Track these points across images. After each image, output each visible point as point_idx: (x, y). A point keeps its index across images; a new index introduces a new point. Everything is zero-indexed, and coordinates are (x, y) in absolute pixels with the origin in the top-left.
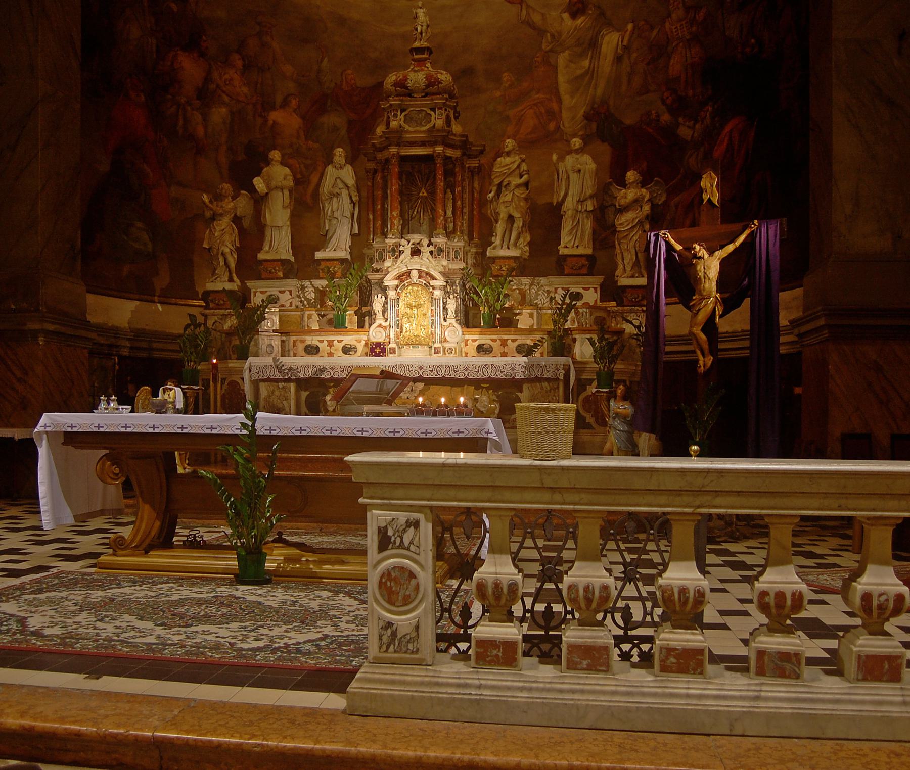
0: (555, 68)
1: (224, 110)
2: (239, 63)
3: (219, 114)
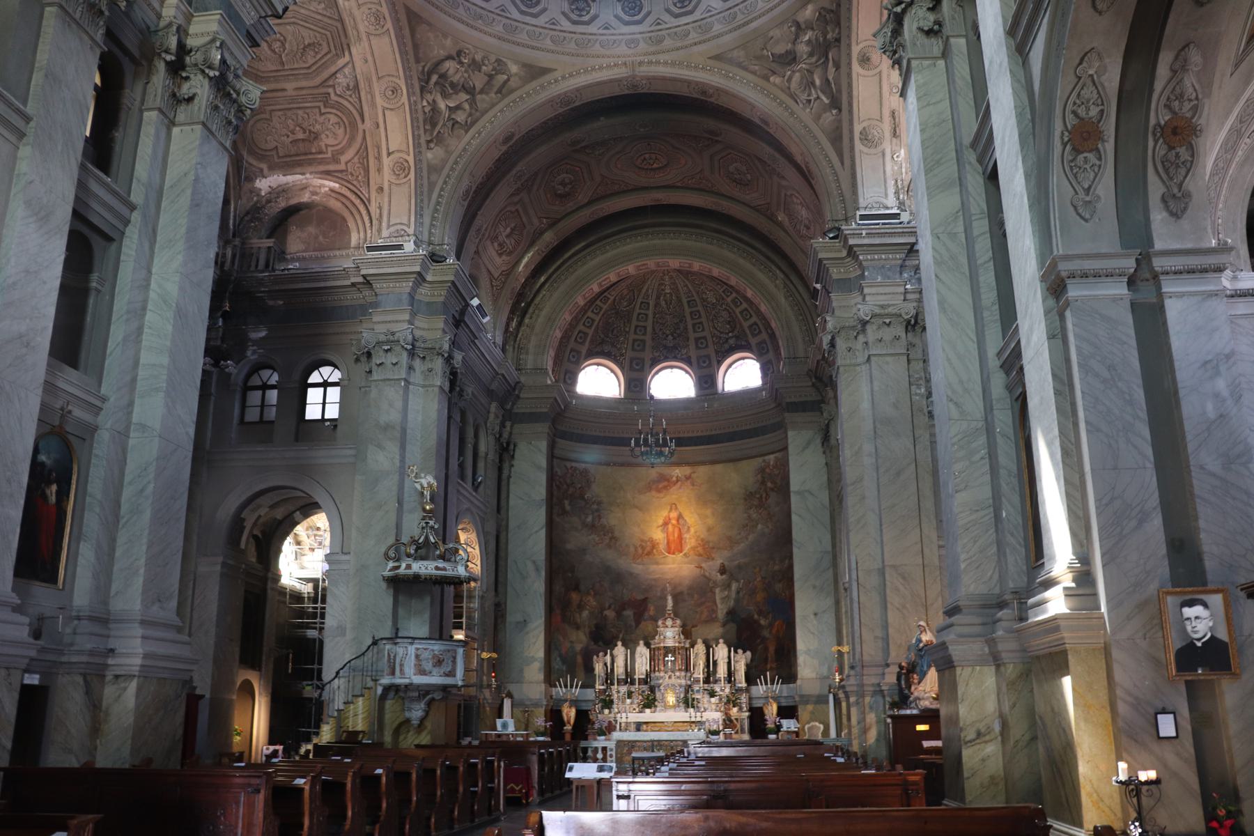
0: (714, 593)
1: (587, 612)
2: (592, 593)
3: (585, 614)
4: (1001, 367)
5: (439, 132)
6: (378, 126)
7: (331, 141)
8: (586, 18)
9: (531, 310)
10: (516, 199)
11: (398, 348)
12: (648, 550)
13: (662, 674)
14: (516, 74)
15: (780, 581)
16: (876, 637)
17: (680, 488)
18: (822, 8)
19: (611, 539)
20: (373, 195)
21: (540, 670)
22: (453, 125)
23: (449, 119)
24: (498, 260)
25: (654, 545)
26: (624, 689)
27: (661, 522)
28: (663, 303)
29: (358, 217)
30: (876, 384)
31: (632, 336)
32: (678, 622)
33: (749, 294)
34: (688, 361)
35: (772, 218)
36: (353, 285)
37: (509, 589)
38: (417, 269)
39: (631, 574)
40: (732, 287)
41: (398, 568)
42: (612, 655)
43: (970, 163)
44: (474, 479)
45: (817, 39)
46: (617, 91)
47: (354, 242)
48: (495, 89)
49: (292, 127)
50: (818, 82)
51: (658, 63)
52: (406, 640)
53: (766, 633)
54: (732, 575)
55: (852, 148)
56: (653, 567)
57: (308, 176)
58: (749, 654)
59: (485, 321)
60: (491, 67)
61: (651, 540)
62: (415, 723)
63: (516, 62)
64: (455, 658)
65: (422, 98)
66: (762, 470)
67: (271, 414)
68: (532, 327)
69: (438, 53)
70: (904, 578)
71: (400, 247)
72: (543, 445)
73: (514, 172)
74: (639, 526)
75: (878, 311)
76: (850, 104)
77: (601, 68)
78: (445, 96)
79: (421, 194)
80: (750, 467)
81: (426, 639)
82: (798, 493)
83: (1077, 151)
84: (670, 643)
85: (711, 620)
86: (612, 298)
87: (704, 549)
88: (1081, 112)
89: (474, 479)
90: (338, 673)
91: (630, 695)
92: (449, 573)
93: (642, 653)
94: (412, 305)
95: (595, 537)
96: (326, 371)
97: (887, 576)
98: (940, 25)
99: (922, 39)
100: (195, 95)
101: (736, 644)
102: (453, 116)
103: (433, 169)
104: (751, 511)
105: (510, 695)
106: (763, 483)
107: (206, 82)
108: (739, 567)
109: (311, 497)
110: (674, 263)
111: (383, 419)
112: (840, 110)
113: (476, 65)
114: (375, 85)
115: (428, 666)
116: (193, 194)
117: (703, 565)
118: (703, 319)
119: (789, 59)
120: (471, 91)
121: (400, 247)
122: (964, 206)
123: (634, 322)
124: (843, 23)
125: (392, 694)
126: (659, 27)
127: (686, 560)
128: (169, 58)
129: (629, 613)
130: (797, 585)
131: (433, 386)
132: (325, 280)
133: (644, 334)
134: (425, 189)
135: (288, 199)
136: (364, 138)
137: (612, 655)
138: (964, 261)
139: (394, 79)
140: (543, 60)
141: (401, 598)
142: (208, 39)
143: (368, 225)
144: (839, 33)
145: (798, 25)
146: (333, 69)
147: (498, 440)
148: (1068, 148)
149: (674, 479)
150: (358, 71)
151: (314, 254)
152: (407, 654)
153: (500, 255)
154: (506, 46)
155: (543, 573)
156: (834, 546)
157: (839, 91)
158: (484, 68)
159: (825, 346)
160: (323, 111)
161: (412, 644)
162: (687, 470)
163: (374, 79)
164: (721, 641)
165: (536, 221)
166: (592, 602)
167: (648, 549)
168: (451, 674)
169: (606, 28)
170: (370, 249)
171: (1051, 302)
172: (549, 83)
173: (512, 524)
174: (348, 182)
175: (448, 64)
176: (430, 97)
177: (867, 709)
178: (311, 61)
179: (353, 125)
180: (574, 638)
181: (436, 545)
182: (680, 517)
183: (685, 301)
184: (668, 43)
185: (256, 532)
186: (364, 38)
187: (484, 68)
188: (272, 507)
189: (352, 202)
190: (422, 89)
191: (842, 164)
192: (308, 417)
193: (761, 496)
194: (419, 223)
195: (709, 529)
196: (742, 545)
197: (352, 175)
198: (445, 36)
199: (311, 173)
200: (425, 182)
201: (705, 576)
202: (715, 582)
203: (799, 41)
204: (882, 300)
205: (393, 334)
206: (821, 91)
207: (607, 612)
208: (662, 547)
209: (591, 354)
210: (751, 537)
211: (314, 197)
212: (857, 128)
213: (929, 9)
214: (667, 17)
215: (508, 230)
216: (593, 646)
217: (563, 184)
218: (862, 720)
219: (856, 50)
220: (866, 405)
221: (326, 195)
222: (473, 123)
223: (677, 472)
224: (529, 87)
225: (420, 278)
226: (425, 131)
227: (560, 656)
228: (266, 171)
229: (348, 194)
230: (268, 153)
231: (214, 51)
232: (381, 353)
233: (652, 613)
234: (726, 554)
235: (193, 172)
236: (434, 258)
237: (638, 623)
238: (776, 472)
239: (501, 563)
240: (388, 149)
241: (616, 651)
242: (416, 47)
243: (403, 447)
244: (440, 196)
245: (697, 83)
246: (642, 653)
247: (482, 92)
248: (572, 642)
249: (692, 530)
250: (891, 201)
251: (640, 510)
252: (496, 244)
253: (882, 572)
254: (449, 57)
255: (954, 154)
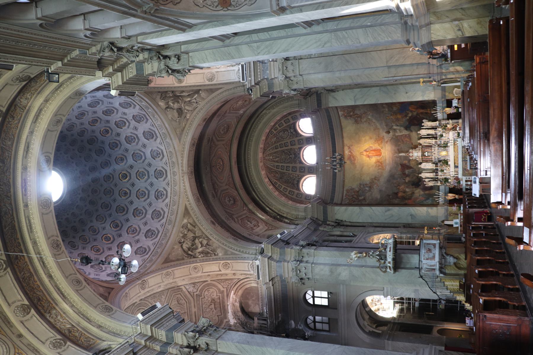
3: (407, 190)
4: (310, 27)
5: (211, 251)
6: (209, 275)
7: (215, 294)
8: (165, 192)
9: (281, 214)
10: (236, 220)
11: (299, 267)
12: (380, 164)
13: (433, 157)
14: (188, 220)
15: (392, 108)
16: (417, 68)
17: (353, 151)
18: (160, 98)
19: (375, 180)
20: (236, 277)
21: (432, 209)
22: (208, 245)
23: (206, 247)
24: (261, 227)
25: (378, 161)
26: (440, 173)
27: (368, 159)
28: (277, 159)
29: (245, 283)
30: (311, 72)
31: (290, 172)
32: (411, 151)
33: (272, 124)
34: (300, 149)
35: (242, 116)
36: (273, 285)
37: (397, 222)
38: (266, 259)
39: (390, 171)
40: (270, 131)
41: (390, 267)
42: (425, 178)
43: (230, 42)
44: (351, 236)
45: (172, 100)
46: (193, 180)
47: (255, 285)
48: (194, 228)
49: (209, 309)
50: (189, 99)
51: (182, 163)
52: (420, 264)
53: (415, 114)
54: (390, 128)
55: (215, 85)
56: (387, 162)
57: (229, 303)
58: (424, 121)
59: (286, 232)
60: (185, 230)
61: (376, 163)
62: (455, 260)
63: (183, 220)
64: (428, 244)
65: (198, 257)
66: (346, 117)
67: (325, 319)
68: (288, 213)
69: (180, 251)
70: (392, 58)
71: (258, 266)
72: (337, 208)
73: (226, 221)
74: (370, 168)
75: (281, 72)
76: (198, 86)
77: (184, 186)
78: (197, 248)
79: (236, 258)
80: (344, 122)
81: (420, 256)
82: (355, 101)
83: (230, 5)
84: (420, 154)
85: (409, 137)
86: (275, 180)
87: (379, 140)
88: (216, 4)
89: (351, 236)
90: (434, 293)
91: (442, 171)
92: (392, 246)
93: (424, 166)
94: (281, 261)
95: (375, 186)
96: (309, 297)
97: (391, 65)
98: (176, 55)
99: (181, 62)
100: (206, 343)
101: (420, 126)
102: (205, 245)
103: (226, 253)
104: (363, 121)
105: (443, 221)
106: (351, 116)
107: (200, 338)
108: (387, 125)
109: (360, 304)
110: (260, 155)
111: (328, 273)
112: (200, 90)
113: (185, 236)
114: (193, 276)
115: (431, 255)
116: (244, 344)
117: (386, 141)
118: (283, 142)
119: (180, 111)
120: (195, 238)
121: (258, 266)
122: (247, 43)
123: (285, 171)
124: (166, 90)
125: (443, 270)
126: (168, 163)
127: (384, 148)
128: (192, 351)
129: (407, 172)
130: (394, 101)
131: (314, 253)
132: (271, 297)
133: (289, 167)
134: (234, 256)
135: (238, 312)
136: (214, 281)
137: (425, 178)
138: (268, 43)
139: (191, 269)
140: (181, 210)
141: (402, 266)
142: (184, 337)
143: (248, 279)
144: (170, 91)
145: (167, 108)
146: (187, 293)
147: (335, 227)
148: (229, 8)
149: (350, 153)
150: (187, 283)
151: (260, 301)
152: (426, 263)
153: (259, 226)
154: (177, 224)
155: (391, 208)
156: (377, 86)
157: (193, 90)
158: (185, 233)
159: (296, 93)
160: (203, 297)
161: (422, 261)
162: (346, 148)
163: (191, 276)
164: (418, 132)
165: (245, 212)
166: (402, 187)
167: (379, 164)
168: (434, 245)
169: (169, 184)
170: (259, 278)
171: (288, 11)
172: (191, 207)
173: (370, 221)
174: (231, 287)
175: (184, 247)
176: (197, 254)
177: (448, 71)
178: (184, 301)
179: (209, 285)
180: (418, 195)
181: (380, 252)
182: (366, 151)
183: (276, 150)
184: (174, 160)
185: (374, 327)
186: (175, 280)
187: (185, 233)
188: (364, 319)
189: (239, 286)
190: (194, 257)
191: (221, 88)
192: (327, 304)
193: (357, 117)
194: (248, 259)
195: (371, 138)
196: (377, 124)
197: (228, 286)
198: (173, 248)
199: (228, 302)
200: (231, 256)
201: (391, 140)
202: (394, 135)
203: (173, 107)
204: (277, 70)
205: (293, 269)
206: (193, 97)
207: (407, 181)
208: (378, 158)
209: (298, 189)
210: (374, 121)
211: (237, 301)
212: (207, 83)
213: (170, 60)
214: (164, 160)
215: (249, 223)
216: (422, 186)
217: (230, 201)
218: (453, 73)
219: (177, 85)
220: (320, 76)
221: (236, 296)
222: (207, 237)
223: (347, 152)
224: (193, 215)
225: (270, 258)
226: (211, 256)
227: (425, 200)
228: (227, 320)
229: (236, 287)
230: (220, 319)
231: (189, 335)
232: (301, 274)
233: (407, 162)
234: (381, 131)
235: (236, 344)
236: (262, 252)
237: (411, 168)
238: (346, 111)
239: (386, 225)
240: (218, 271)
241: (424, 177)
242: (178, 260)
243: (339, 265)
244: (236, 250)
245: (190, 147)
246: (424, 166)
247: (195, 234)
248: (420, 195)
249: (371, 145)
250: (236, 68)
251: (363, 167)
252: (254, 228)
253: (389, 67)
254: (182, 246)
255: (226, 48)
